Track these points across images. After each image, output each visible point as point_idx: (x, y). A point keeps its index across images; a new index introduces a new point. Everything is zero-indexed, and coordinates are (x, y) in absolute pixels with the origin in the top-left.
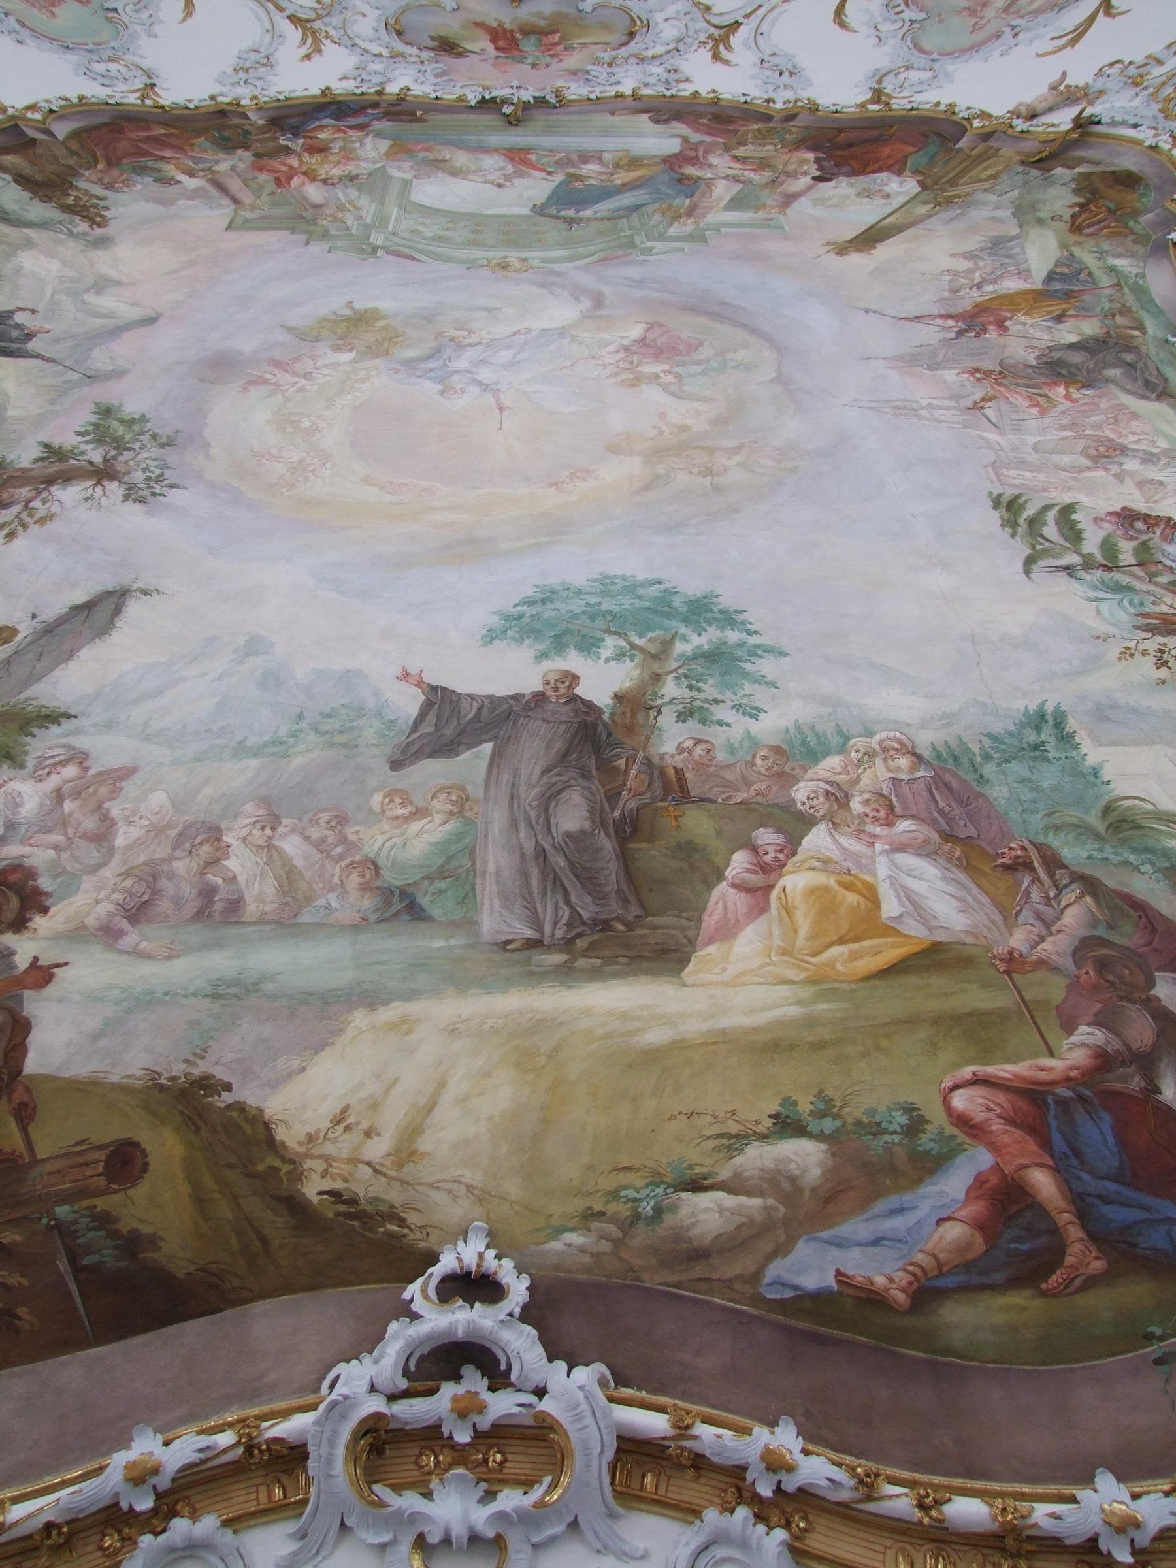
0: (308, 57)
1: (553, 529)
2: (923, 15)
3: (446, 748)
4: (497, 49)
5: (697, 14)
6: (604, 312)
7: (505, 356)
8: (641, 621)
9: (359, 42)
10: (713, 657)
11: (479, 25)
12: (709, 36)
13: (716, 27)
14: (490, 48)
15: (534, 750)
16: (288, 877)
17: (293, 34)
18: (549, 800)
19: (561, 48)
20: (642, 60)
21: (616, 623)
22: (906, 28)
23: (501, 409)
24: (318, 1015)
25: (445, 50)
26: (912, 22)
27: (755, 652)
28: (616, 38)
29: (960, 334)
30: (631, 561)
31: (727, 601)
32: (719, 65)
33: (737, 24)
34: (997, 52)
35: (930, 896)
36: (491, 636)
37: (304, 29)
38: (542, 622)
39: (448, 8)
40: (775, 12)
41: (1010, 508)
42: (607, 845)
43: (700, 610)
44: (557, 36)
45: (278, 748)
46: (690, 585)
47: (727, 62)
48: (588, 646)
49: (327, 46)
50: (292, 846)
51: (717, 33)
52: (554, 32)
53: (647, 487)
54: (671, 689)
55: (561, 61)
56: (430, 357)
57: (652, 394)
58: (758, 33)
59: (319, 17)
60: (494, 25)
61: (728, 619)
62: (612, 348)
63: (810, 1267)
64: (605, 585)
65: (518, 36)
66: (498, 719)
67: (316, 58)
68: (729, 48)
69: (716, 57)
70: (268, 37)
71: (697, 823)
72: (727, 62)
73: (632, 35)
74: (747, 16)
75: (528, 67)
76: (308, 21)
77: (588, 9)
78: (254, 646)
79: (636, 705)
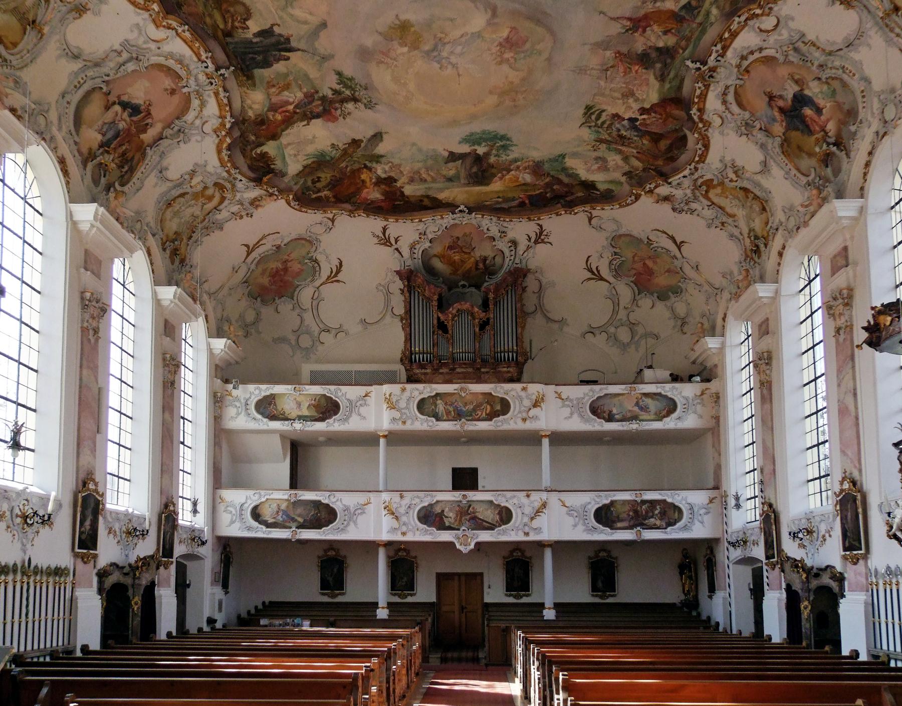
1: (473, 117)
3: (454, 161)
6: (495, 21)
7: (459, 49)
8: (491, 139)
10: (503, 146)
15: (469, 161)
16: (432, 178)
18: (471, 168)
21: (485, 140)
23: (459, 75)
24: (441, 190)
27: (512, 145)
29: (627, 31)
30: (490, 126)
31: (509, 136)
35: (528, 178)
36: (460, 143)
38: (471, 139)
41: (588, 108)
42: (480, 173)
43: (503, 137)
45: (425, 161)
46: (502, 133)
48: (479, 144)
50: (432, 174)
53: (498, 105)
54: (494, 152)
56: (433, 50)
57: (505, 68)
61: (508, 139)
62: (496, 44)
63: (498, 206)
64: (484, 132)
66: (462, 157)
71: (494, 171)
78: (414, 144)
79: (487, 154)
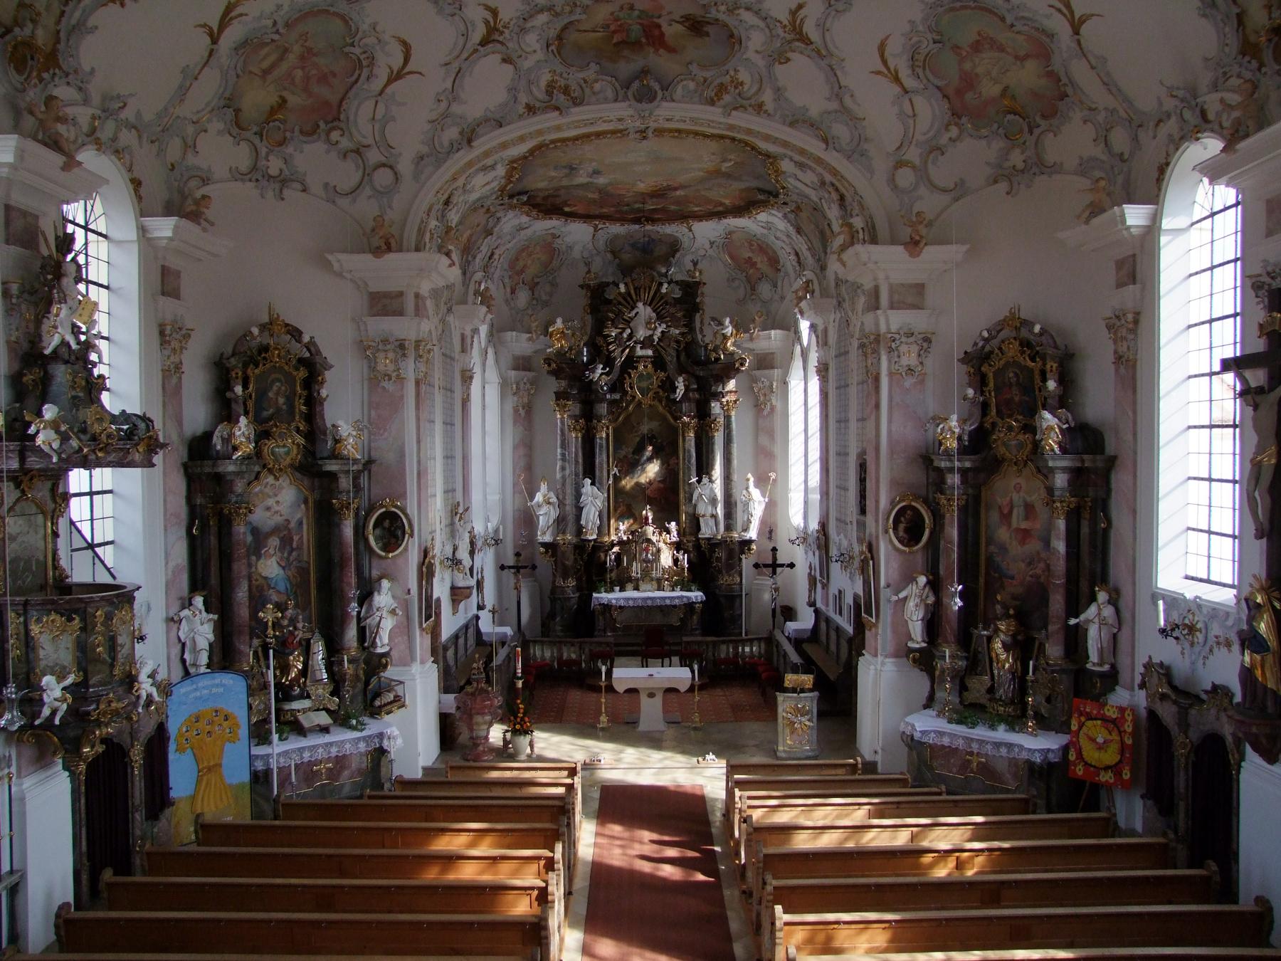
0: (800, 7)
2: (347, 49)
4: (659, 26)
5: (514, 57)
9: (762, 24)
11: (671, 50)
12: (502, 33)
13: (498, 41)
14: (665, 28)
17: (810, 29)
19: (612, 28)
20: (550, 9)
22: (357, 38)
25: (699, 22)
26: (352, 45)
28: (573, 36)
32: (492, 5)
33: (484, 43)
34: (286, 8)
37: (801, 33)
39: (695, 65)
40: (456, 53)
44: (615, 41)
47: (487, 8)
49: (784, 17)
51: (496, 37)
52: (615, 45)
55: (612, 14)
58: (466, 35)
59: (790, 42)
60: (662, 51)
65: (644, 40)
67: (794, 7)
68: (487, 22)
69: (495, 13)
70: (828, 25)
72: (487, 8)
73: (559, 38)
74: (476, 51)
75: (638, 6)
76: (798, 40)
77: (592, 65)
